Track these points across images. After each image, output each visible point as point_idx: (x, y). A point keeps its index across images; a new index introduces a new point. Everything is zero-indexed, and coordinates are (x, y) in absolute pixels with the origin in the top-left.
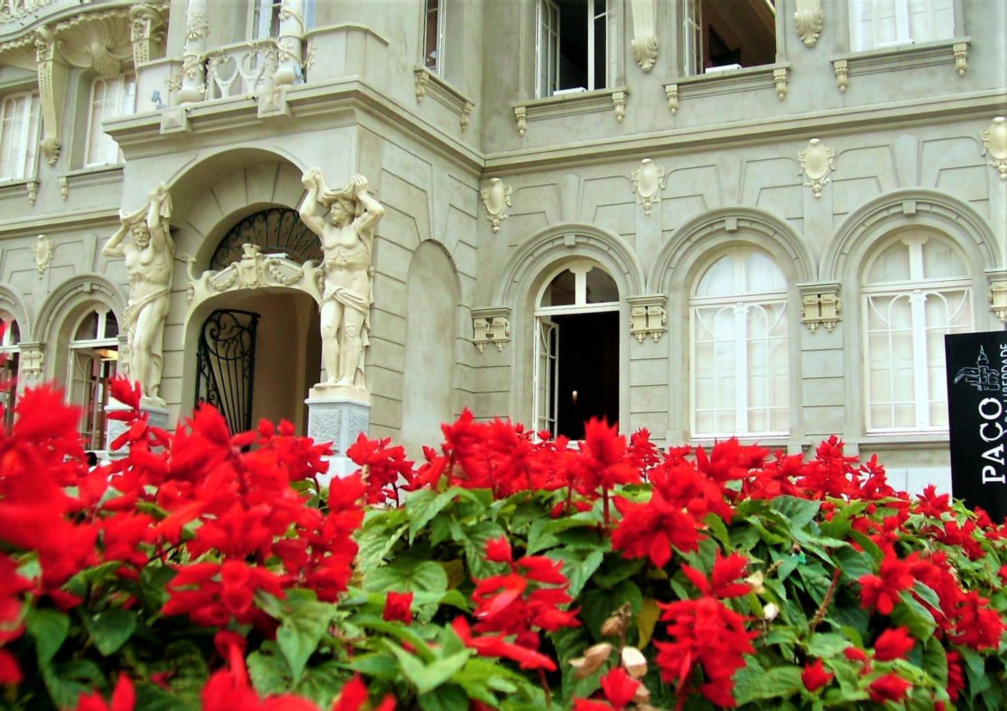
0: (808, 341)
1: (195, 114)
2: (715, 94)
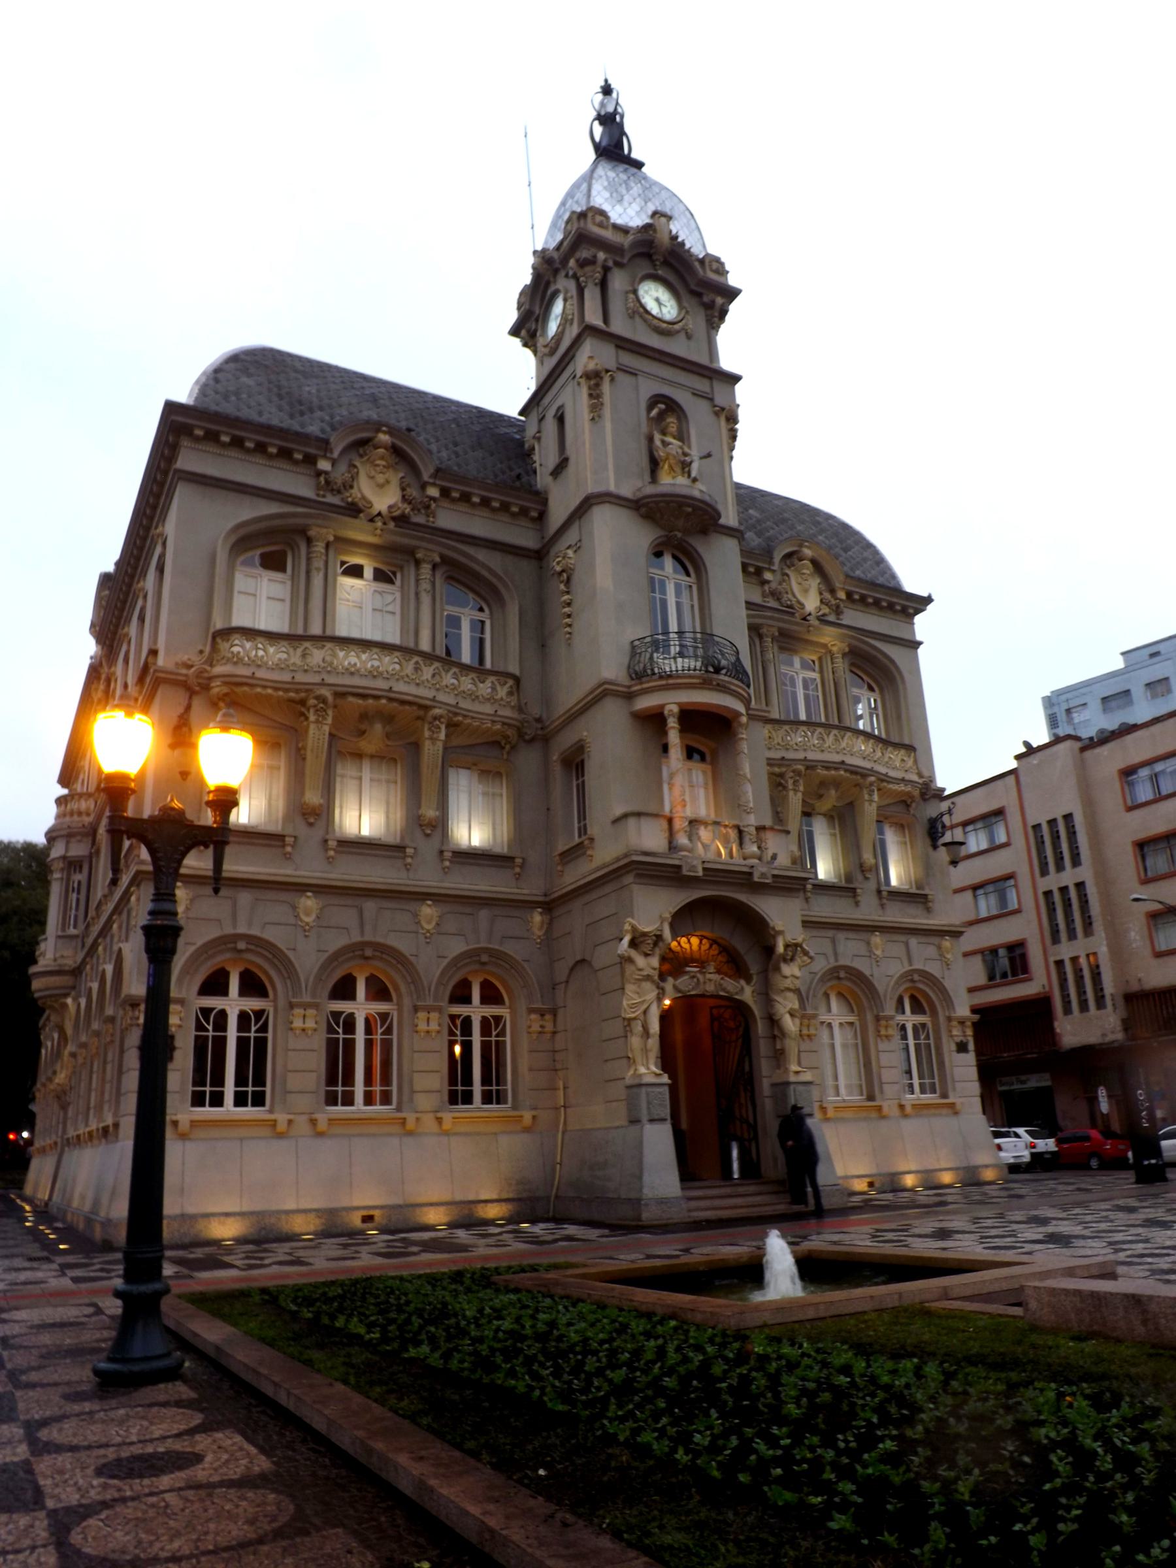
1: (707, 866)
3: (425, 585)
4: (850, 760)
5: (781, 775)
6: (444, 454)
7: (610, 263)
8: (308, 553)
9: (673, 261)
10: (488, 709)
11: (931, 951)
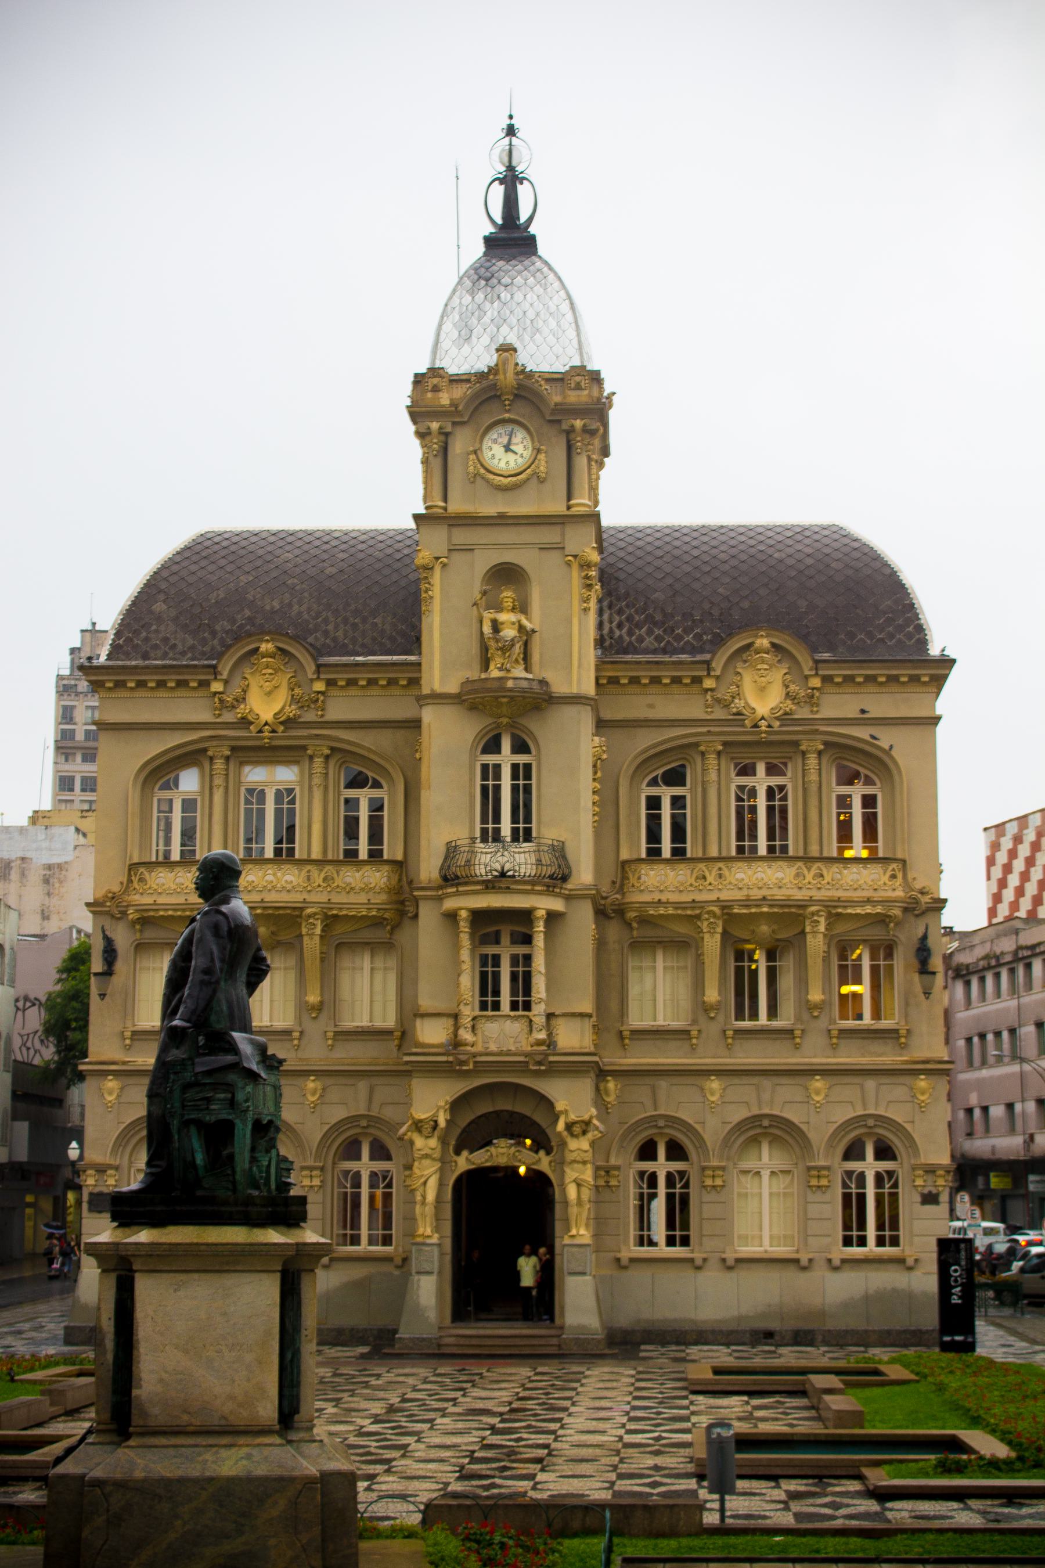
0: (811, 1197)
2: (756, 1039)
3: (317, 780)
5: (698, 917)
6: (340, 634)
7: (449, 429)
8: (211, 770)
9: (523, 393)
10: (362, 898)
11: (899, 1092)
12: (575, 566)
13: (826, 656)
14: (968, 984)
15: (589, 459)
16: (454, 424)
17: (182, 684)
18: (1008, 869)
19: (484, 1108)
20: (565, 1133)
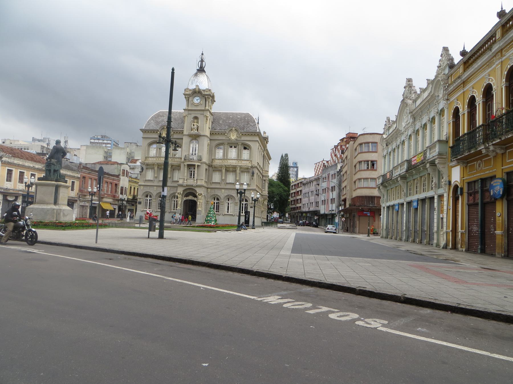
0: (235, 206)
4: (231, 164)
5: (222, 167)
6: (176, 126)
7: (189, 97)
12: (205, 117)
13: (242, 131)
14: (304, 186)
15: (209, 102)
16: (190, 96)
17: (154, 132)
18: (317, 170)
19: (188, 191)
20: (198, 195)
